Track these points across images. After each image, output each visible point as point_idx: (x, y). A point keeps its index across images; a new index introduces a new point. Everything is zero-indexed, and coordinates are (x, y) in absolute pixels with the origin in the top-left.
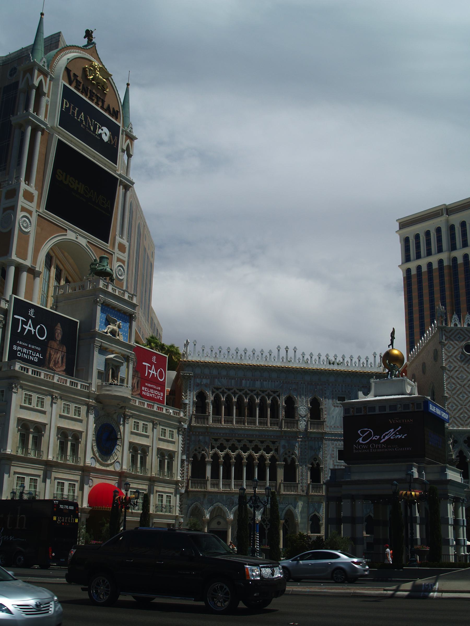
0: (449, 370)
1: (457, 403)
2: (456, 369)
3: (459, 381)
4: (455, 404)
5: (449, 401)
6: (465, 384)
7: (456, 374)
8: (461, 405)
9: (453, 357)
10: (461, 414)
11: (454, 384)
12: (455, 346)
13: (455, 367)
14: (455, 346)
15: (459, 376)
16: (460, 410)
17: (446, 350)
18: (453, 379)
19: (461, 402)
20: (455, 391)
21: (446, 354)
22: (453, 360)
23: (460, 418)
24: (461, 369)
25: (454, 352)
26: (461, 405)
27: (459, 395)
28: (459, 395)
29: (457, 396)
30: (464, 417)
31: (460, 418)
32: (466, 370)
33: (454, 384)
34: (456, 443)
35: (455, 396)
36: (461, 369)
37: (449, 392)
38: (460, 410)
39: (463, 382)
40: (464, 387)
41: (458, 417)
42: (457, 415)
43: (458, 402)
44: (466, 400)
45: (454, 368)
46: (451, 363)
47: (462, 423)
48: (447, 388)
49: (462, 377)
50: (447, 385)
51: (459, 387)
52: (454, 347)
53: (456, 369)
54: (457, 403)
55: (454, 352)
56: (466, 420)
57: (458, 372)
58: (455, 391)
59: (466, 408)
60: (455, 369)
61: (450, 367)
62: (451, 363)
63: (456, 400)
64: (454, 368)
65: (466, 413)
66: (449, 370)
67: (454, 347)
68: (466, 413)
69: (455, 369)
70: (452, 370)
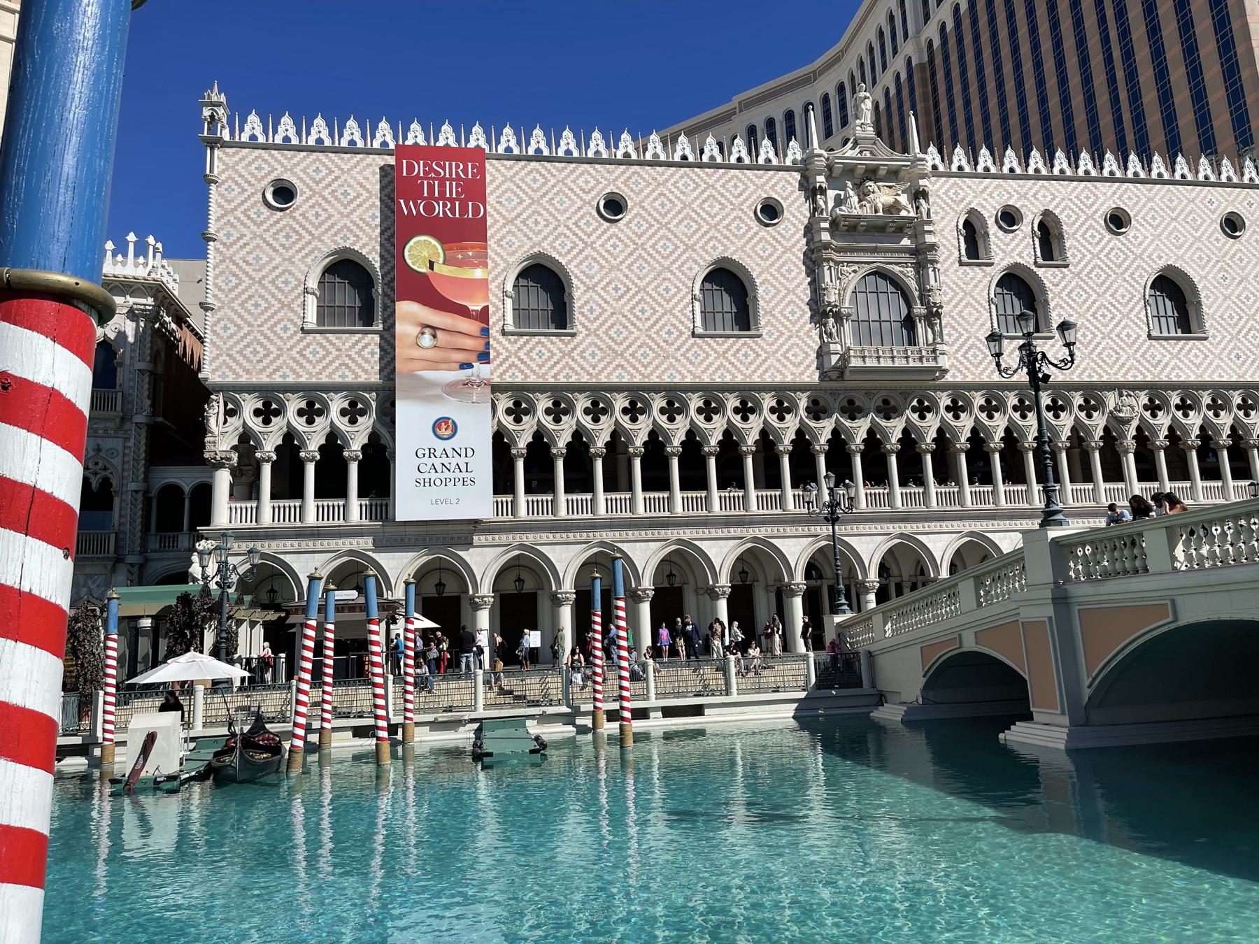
0: (224, 244)
1: (239, 321)
2: (244, 240)
3: (247, 268)
4: (232, 321)
5: (219, 315)
6: (264, 277)
7: (244, 252)
8: (250, 325)
9: (238, 213)
10: (248, 346)
11: (235, 275)
12: (246, 186)
13: (243, 236)
14: (246, 186)
15: (250, 258)
16: (245, 336)
17: (222, 196)
18: (237, 265)
19: (250, 318)
20: (236, 292)
21: (220, 206)
22: (238, 219)
23: (245, 356)
24: (258, 241)
25: (242, 203)
26: (250, 325)
27: (246, 301)
28: (246, 301)
29: (242, 305)
30: (255, 352)
31: (245, 356)
32: (268, 244)
33: (235, 275)
34: (231, 416)
35: (235, 305)
36: (258, 241)
37: (220, 295)
38: (245, 336)
39: (260, 270)
40: (260, 282)
41: (240, 352)
42: (238, 348)
43: (243, 319)
44: (262, 313)
45: (239, 239)
46: (232, 225)
47: (248, 366)
48: (215, 284)
49: (258, 259)
50: (216, 277)
51: (248, 281)
52: (244, 190)
53: (244, 240)
54: (239, 321)
55: (242, 203)
56: (260, 361)
57: (248, 248)
58: (236, 292)
59: (262, 333)
60: (241, 242)
61: (228, 235)
62: (232, 225)
63: (236, 312)
64: (239, 239)
65: (260, 343)
66: (224, 244)
67: (244, 190)
68: (260, 343)
69: (241, 242)
70: (232, 244)
